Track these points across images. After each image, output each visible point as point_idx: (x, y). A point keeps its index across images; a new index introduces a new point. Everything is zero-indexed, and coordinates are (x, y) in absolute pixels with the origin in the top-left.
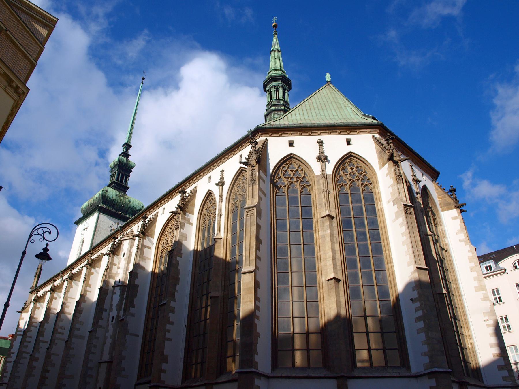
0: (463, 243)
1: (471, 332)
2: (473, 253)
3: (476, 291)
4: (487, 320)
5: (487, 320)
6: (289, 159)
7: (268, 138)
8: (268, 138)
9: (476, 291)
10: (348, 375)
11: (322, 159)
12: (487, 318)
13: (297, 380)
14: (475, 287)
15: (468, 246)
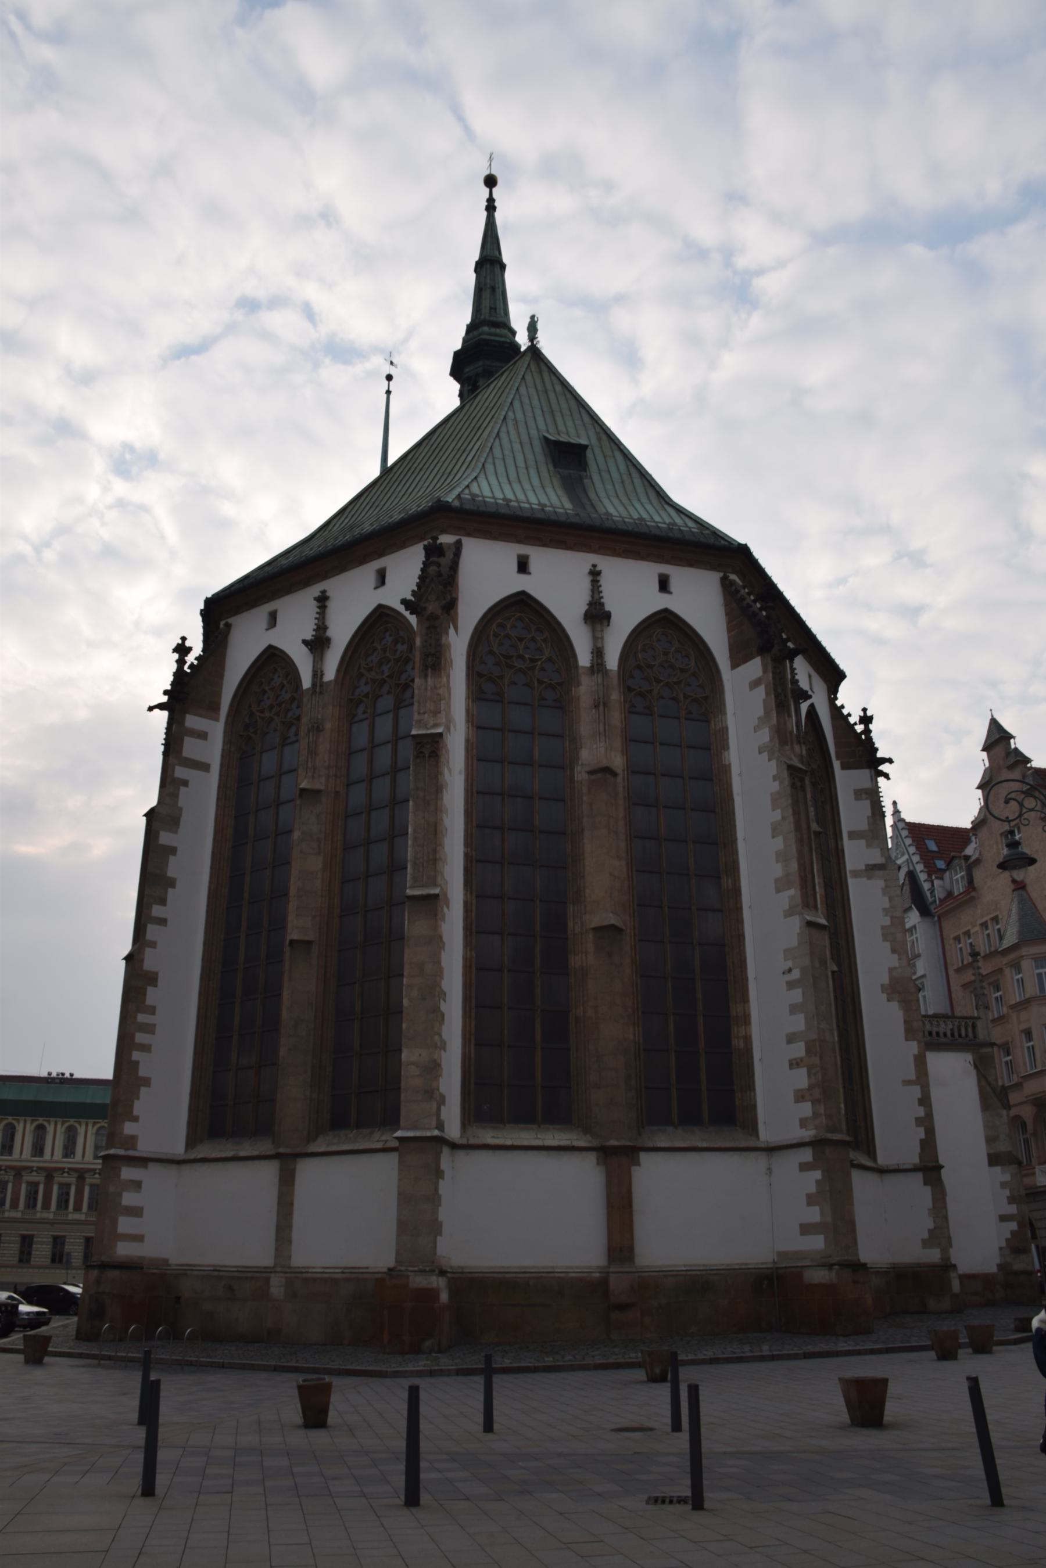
0: (765, 755)
1: (749, 1008)
2: (781, 783)
3: (778, 890)
4: (790, 971)
5: (790, 971)
6: (272, 659)
7: (230, 620)
8: (230, 620)
9: (778, 890)
10: (298, 1150)
11: (318, 644)
12: (790, 964)
13: (220, 1165)
14: (776, 880)
15: (774, 762)
